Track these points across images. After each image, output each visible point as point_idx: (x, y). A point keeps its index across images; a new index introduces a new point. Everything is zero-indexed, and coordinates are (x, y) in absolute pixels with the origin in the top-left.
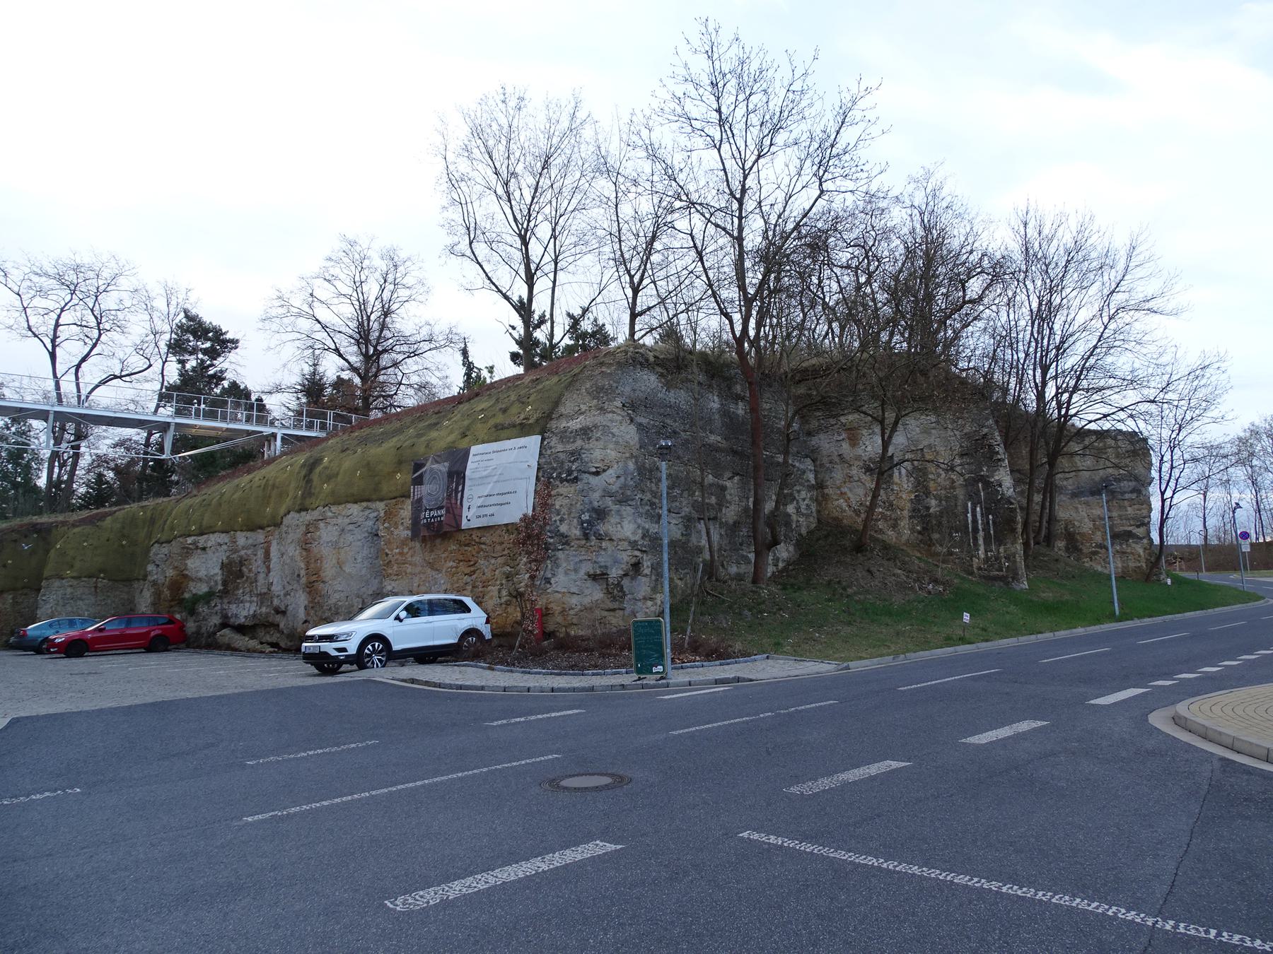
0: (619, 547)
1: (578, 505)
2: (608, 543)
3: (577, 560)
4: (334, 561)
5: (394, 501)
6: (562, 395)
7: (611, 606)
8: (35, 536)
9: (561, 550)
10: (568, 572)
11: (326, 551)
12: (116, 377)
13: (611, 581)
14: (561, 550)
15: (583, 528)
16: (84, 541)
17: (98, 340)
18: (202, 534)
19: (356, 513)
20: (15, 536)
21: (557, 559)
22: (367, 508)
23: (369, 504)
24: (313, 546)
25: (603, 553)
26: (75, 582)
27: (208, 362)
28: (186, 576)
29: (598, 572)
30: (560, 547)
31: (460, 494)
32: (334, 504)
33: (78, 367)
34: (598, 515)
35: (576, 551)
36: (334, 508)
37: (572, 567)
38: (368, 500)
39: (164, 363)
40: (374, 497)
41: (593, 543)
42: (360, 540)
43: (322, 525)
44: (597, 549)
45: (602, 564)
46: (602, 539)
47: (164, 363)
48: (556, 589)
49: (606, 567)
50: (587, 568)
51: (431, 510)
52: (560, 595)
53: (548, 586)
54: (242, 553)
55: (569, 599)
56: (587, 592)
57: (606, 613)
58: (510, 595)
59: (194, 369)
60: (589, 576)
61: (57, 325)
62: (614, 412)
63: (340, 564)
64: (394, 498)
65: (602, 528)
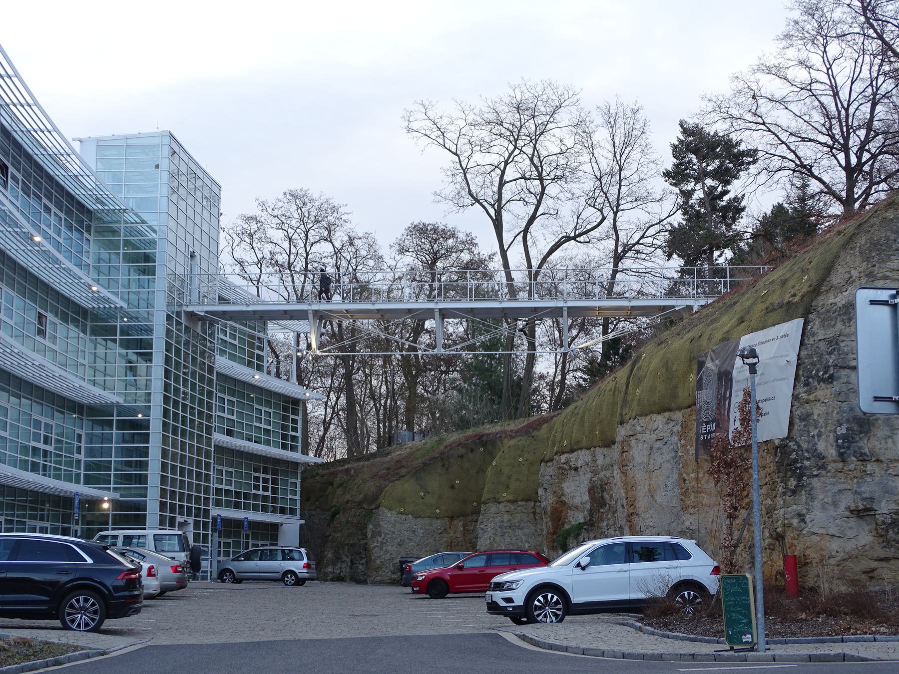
0: (890, 471)
1: (835, 414)
2: (875, 465)
3: (836, 489)
4: (647, 488)
5: (689, 409)
6: (837, 257)
7: (882, 553)
8: (482, 449)
9: (816, 476)
10: (826, 506)
11: (638, 475)
12: (568, 239)
13: (880, 519)
14: (816, 476)
15: (838, 446)
16: (520, 456)
17: (543, 193)
18: (572, 451)
19: (661, 427)
20: (462, 451)
21: (812, 489)
22: (670, 419)
23: (671, 414)
24: (629, 468)
25: (869, 479)
26: (512, 507)
27: (720, 189)
28: (563, 503)
29: (861, 507)
30: (815, 473)
31: (727, 402)
32: (641, 416)
33: (526, 231)
34: (861, 426)
35: (834, 477)
36: (642, 421)
37: (829, 500)
38: (670, 410)
39: (615, 214)
40: (673, 405)
41: (852, 467)
42: (668, 461)
43: (633, 442)
44: (859, 474)
45: (867, 495)
46: (865, 460)
47: (615, 214)
48: (812, 530)
49: (872, 499)
50: (847, 501)
51: (707, 423)
52: (818, 538)
53: (803, 525)
54: (602, 475)
55: (828, 544)
56: (850, 533)
57: (874, 564)
58: (771, 536)
59: (701, 202)
60: (852, 512)
61: (502, 184)
62: (886, 278)
63: (652, 493)
64: (689, 407)
65: (866, 445)
